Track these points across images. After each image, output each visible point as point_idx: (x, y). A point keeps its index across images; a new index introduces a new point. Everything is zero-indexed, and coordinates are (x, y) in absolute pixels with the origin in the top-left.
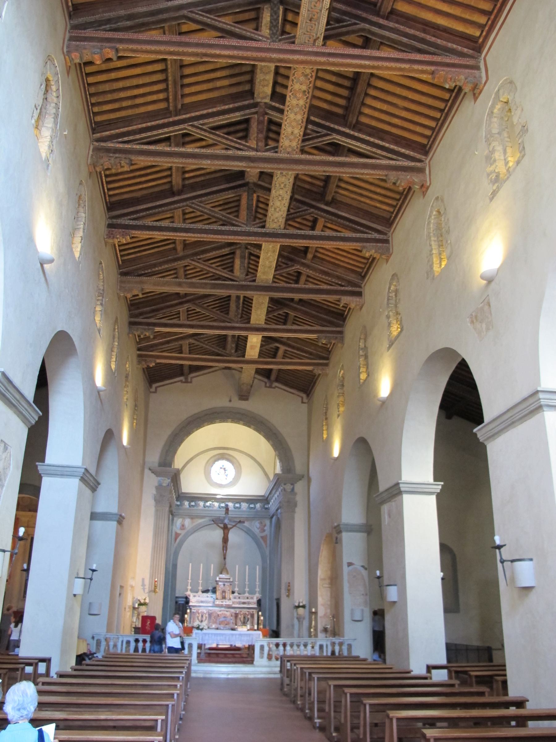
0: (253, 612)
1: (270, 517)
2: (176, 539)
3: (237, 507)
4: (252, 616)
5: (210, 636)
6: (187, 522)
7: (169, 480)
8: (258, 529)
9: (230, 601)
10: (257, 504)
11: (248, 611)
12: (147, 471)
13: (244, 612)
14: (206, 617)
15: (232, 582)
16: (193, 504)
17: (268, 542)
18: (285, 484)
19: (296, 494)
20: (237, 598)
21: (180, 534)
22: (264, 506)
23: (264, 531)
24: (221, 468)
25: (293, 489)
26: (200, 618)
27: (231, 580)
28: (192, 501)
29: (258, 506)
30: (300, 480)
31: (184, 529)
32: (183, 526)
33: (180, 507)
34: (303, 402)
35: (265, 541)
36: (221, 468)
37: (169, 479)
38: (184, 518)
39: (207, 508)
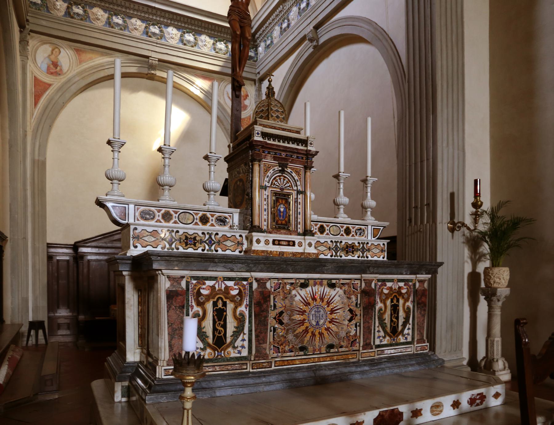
3: (189, 42)
9: (309, 239)
11: (405, 281)
13: (395, 286)
14: (240, 320)
38: (56, 47)
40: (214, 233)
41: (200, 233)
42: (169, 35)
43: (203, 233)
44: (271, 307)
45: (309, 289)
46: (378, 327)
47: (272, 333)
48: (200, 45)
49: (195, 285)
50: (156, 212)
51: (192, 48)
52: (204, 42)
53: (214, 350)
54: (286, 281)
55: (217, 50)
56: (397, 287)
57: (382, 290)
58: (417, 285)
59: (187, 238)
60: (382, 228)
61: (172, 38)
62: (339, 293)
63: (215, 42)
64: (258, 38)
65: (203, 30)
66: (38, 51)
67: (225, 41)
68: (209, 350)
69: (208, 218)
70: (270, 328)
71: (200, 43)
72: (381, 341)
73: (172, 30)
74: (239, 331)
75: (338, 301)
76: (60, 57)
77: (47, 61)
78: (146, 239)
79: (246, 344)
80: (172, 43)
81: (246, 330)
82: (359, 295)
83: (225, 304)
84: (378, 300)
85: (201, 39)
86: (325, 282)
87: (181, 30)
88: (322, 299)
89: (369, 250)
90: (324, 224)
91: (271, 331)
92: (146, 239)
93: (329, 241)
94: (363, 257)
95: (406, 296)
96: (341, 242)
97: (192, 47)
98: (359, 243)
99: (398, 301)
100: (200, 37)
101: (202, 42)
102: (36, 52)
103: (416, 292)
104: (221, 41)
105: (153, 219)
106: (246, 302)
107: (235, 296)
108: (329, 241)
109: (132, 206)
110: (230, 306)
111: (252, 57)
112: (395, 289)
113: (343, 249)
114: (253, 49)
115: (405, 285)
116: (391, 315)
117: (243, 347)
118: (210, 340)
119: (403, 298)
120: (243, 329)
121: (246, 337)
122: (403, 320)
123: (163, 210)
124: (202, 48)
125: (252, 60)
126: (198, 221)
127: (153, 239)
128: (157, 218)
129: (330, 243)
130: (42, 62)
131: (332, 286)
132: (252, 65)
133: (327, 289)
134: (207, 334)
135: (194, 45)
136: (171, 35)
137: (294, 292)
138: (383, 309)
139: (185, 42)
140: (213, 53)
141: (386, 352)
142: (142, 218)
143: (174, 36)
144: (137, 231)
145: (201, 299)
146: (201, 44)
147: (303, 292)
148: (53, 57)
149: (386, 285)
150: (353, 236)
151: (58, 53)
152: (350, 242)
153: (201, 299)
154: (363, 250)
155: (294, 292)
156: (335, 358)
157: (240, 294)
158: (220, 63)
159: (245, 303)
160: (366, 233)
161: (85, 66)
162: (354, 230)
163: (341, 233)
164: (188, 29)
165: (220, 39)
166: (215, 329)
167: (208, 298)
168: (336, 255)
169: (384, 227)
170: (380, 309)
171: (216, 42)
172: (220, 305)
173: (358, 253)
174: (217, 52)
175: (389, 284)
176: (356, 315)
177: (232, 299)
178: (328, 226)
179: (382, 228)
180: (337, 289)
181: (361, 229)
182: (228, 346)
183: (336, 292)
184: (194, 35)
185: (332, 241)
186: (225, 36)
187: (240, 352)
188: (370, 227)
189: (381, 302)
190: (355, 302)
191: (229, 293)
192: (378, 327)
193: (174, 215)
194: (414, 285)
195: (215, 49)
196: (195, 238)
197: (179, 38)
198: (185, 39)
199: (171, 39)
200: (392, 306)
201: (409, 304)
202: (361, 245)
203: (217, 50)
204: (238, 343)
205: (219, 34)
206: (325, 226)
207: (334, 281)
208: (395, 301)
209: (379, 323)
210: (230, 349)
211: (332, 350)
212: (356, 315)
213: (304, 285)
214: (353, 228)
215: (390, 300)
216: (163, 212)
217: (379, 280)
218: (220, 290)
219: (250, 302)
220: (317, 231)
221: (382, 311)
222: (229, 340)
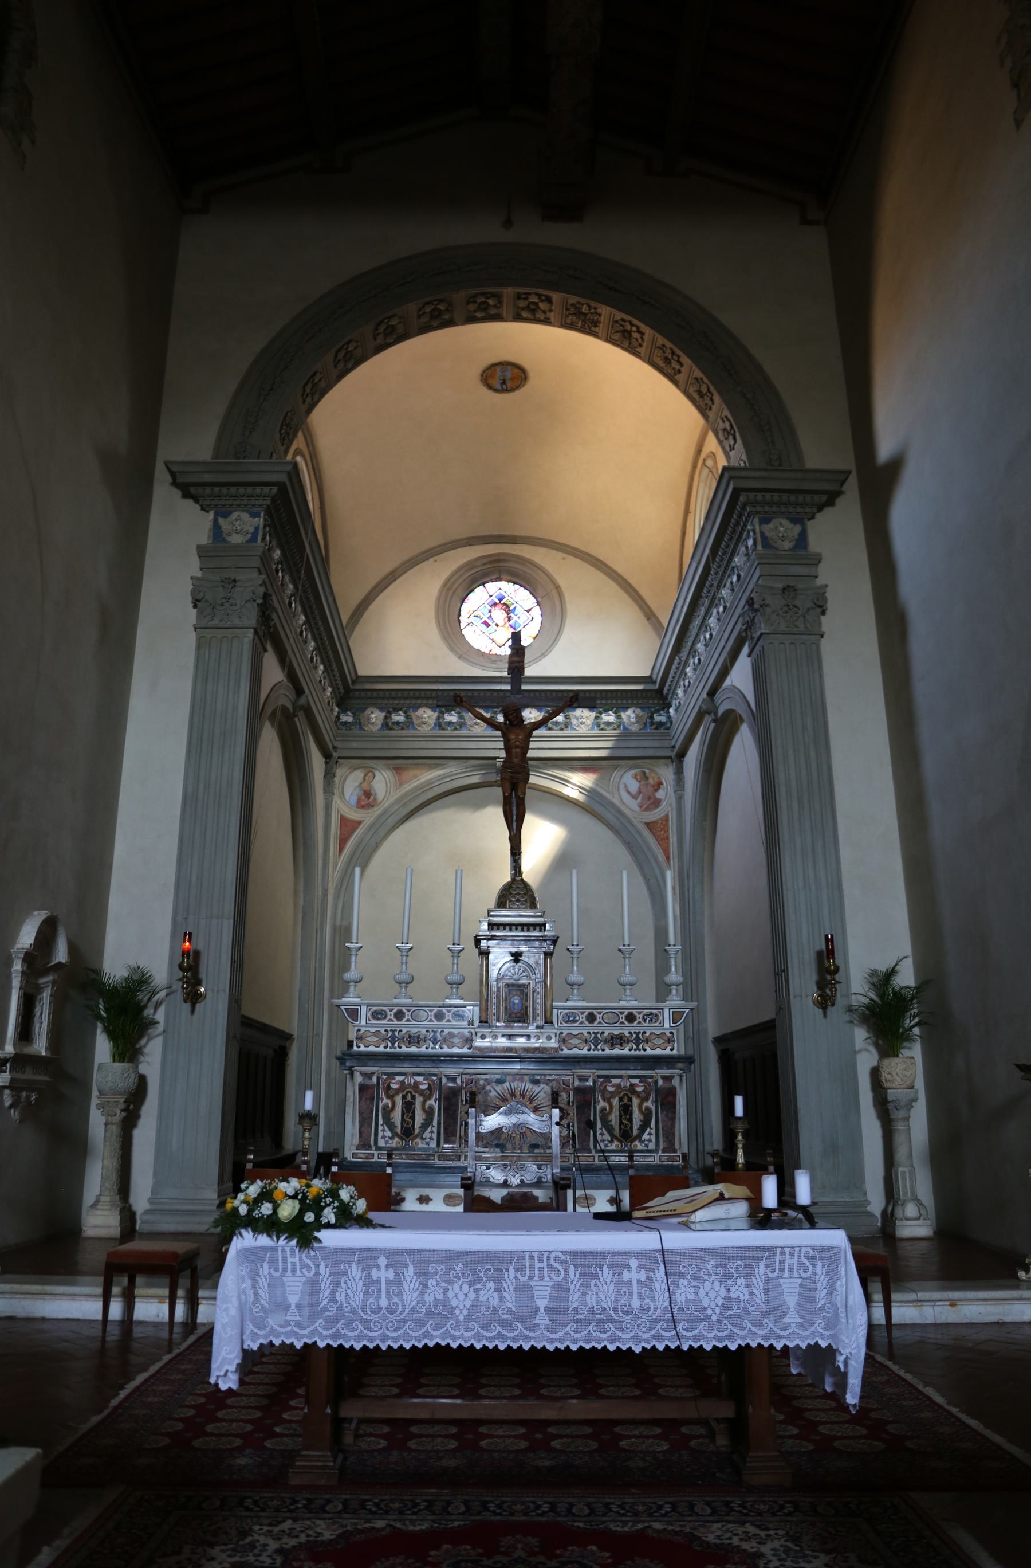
0: (667, 1079)
1: (673, 754)
2: (343, 842)
4: (667, 1099)
5: (383, 1274)
6: (382, 782)
7: (260, 521)
8: (635, 797)
10: (626, 709)
12: (163, 492)
13: (626, 1083)
14: (429, 1113)
15: (554, 941)
16: (399, 717)
17: (673, 839)
18: (765, 521)
19: (816, 560)
20: (582, 1018)
21: (359, 823)
22: (652, 718)
23: (657, 803)
24: (495, 604)
25: (802, 540)
26: (397, 1116)
27: (549, 931)
28: (396, 710)
29: (629, 715)
30: (830, 502)
31: (370, 806)
32: (368, 794)
33: (356, 731)
34: (805, 221)
35: (663, 841)
36: (495, 604)
37: (254, 515)
38: (370, 772)
39: (449, 731)
40: (440, 1030)
41: (424, 1031)
43: (427, 1031)
44: (462, 1101)
45: (507, 1084)
46: (601, 1129)
47: (463, 1127)
49: (385, 1080)
50: (388, 1011)
53: (402, 1139)
54: (479, 1076)
55: (602, 726)
56: (629, 1084)
57: (605, 1087)
58: (660, 1082)
59: (410, 1037)
60: (687, 1011)
62: (545, 1089)
64: (667, 694)
66: (348, 781)
68: (396, 1139)
69: (444, 1014)
70: (461, 1123)
71: (574, 722)
72: (606, 1146)
74: (427, 1123)
75: (544, 1098)
76: (374, 783)
77: (358, 792)
78: (369, 1039)
79: (435, 1136)
81: (435, 1122)
82: (572, 1093)
83: (414, 1097)
84: (600, 1098)
86: (526, 1078)
87: (544, 710)
88: (523, 1096)
89: (647, 1041)
90: (595, 1012)
91: (461, 1125)
92: (369, 1039)
93: (585, 1033)
94: (637, 1049)
95: (643, 1095)
96: (603, 1033)
97: (562, 729)
98: (630, 1033)
99: (630, 1100)
100: (574, 713)
101: (577, 719)
102: (345, 780)
103: (658, 1091)
105: (385, 1018)
106: (436, 1095)
107: (424, 1090)
108: (585, 1033)
109: (364, 1008)
110: (419, 1100)
112: (625, 1087)
113: (606, 1042)
114: (663, 709)
115: (640, 1082)
116: (621, 1116)
117: (431, 1138)
118: (399, 1130)
119: (638, 1096)
120: (432, 1122)
121: (435, 1130)
122: (640, 1123)
123: (396, 1009)
126: (433, 1018)
127: (376, 1039)
128: (389, 1017)
129: (586, 1035)
130: (351, 794)
131: (536, 1082)
133: (529, 1086)
134: (396, 1124)
135: (563, 726)
137: (488, 1088)
138: (608, 1108)
140: (596, 732)
141: (612, 1158)
142: (374, 1018)
144: (360, 1032)
145: (391, 1093)
147: (499, 1088)
148: (365, 786)
149: (611, 1082)
150: (639, 1023)
151: (371, 778)
152: (616, 1033)
153: (391, 1093)
154: (637, 1042)
155: (488, 1088)
156: (539, 1159)
157: (429, 1088)
158: (609, 744)
159: (434, 1097)
160: (661, 1018)
161: (407, 787)
162: (641, 1016)
163: (621, 1020)
165: (607, 707)
166: (403, 1120)
167: (397, 1091)
168: (596, 1049)
169: (692, 1009)
170: (603, 1109)
171: (601, 714)
172: (409, 1098)
173: (630, 1045)
174: (602, 729)
175: (615, 1081)
176: (568, 1114)
177: (422, 1093)
178: (600, 1013)
179: (687, 1011)
180: (542, 1086)
181: (651, 1014)
182: (416, 1137)
183: (540, 1088)
185: (588, 1033)
187: (428, 1144)
188: (666, 1011)
189: (604, 1100)
190: (566, 1100)
191: (418, 1087)
192: (601, 1129)
193: (407, 1013)
194: (656, 1082)
195: (598, 725)
196: (418, 1037)
200: (620, 1106)
201: (649, 1104)
202: (634, 1036)
204: (427, 1134)
206: (596, 1013)
207: (538, 1077)
208: (626, 1101)
209: (602, 1125)
210: (418, 1140)
211: (536, 1151)
212: (568, 1114)
213: (500, 1082)
214: (640, 1013)
215: (617, 1099)
216: (395, 1011)
217: (599, 1076)
218: (409, 1085)
219: (440, 1096)
220: (584, 1019)
221: (605, 1109)
222: (417, 1131)
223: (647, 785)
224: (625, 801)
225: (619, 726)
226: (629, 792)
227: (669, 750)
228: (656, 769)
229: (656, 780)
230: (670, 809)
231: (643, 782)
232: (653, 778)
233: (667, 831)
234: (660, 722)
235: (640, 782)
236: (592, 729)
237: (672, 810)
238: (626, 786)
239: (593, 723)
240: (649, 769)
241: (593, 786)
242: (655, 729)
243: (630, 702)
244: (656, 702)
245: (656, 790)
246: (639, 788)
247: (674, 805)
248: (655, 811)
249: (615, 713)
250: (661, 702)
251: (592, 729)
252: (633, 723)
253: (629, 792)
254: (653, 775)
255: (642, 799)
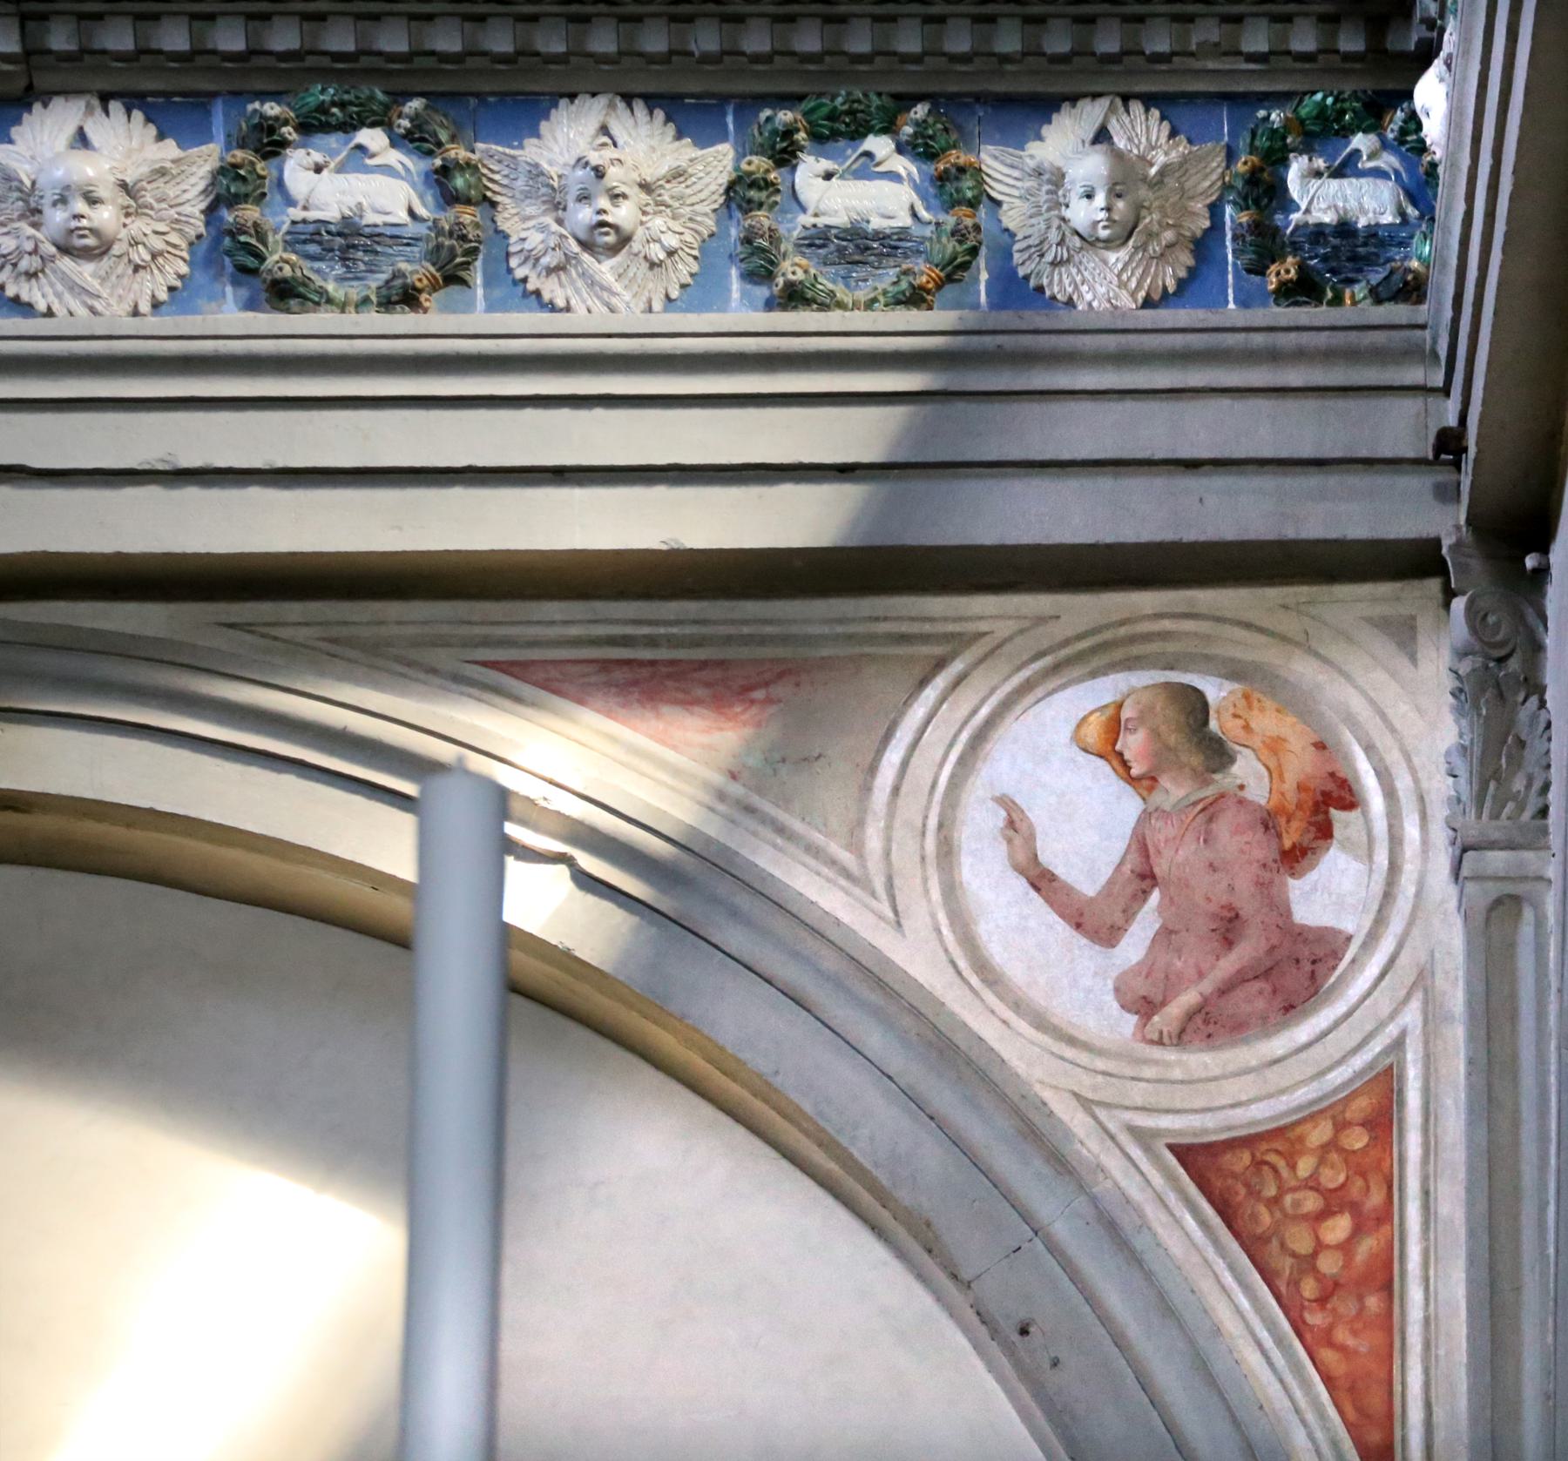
42: (33, 214)
48: (531, 258)
51: (403, 321)
52: (584, 198)
55: (793, 268)
61: (85, 254)
63: (758, 164)
65: (552, 42)
67: (920, 111)
73: (82, 139)
80: (83, 321)
85: (536, 172)
97: (406, 297)
100: (531, 151)
104: (857, 134)
111: (1373, 232)
124: (553, 290)
125: (1360, 290)
132: (1380, 356)
135: (416, 269)
136: (57, 218)
139: (279, 260)
143: (105, 217)
146: (535, 240)
164: (325, 74)
171: (786, 157)
174: (794, 297)
184: (416, 139)
186: (909, 41)
195: (759, 264)
197: (198, 225)
198: (279, 220)
199: (66, 263)
203: (793, 268)
205: (808, 40)
223: (1210, 810)
224: (997, 951)
225: (955, 271)
226: (1041, 880)
227: (1419, 484)
228: (1303, 669)
229: (1300, 764)
230: (1411, 1016)
231: (1174, 791)
232: (1275, 746)
233: (1386, 1215)
234: (1345, 228)
235: (1144, 783)
236: (700, 292)
237: (1433, 1019)
238: (1015, 824)
239: (707, 249)
240: (1234, 671)
241: (713, 828)
242: (1291, 293)
243: (1058, 42)
244: (1304, 39)
245: (1295, 858)
246: (1141, 844)
247: (1456, 999)
248: (1279, 1044)
249: (921, 148)
250: (1351, 42)
251: (700, 292)
252: (1090, 242)
253: (1041, 880)
254: (1267, 722)
255: (1166, 934)
